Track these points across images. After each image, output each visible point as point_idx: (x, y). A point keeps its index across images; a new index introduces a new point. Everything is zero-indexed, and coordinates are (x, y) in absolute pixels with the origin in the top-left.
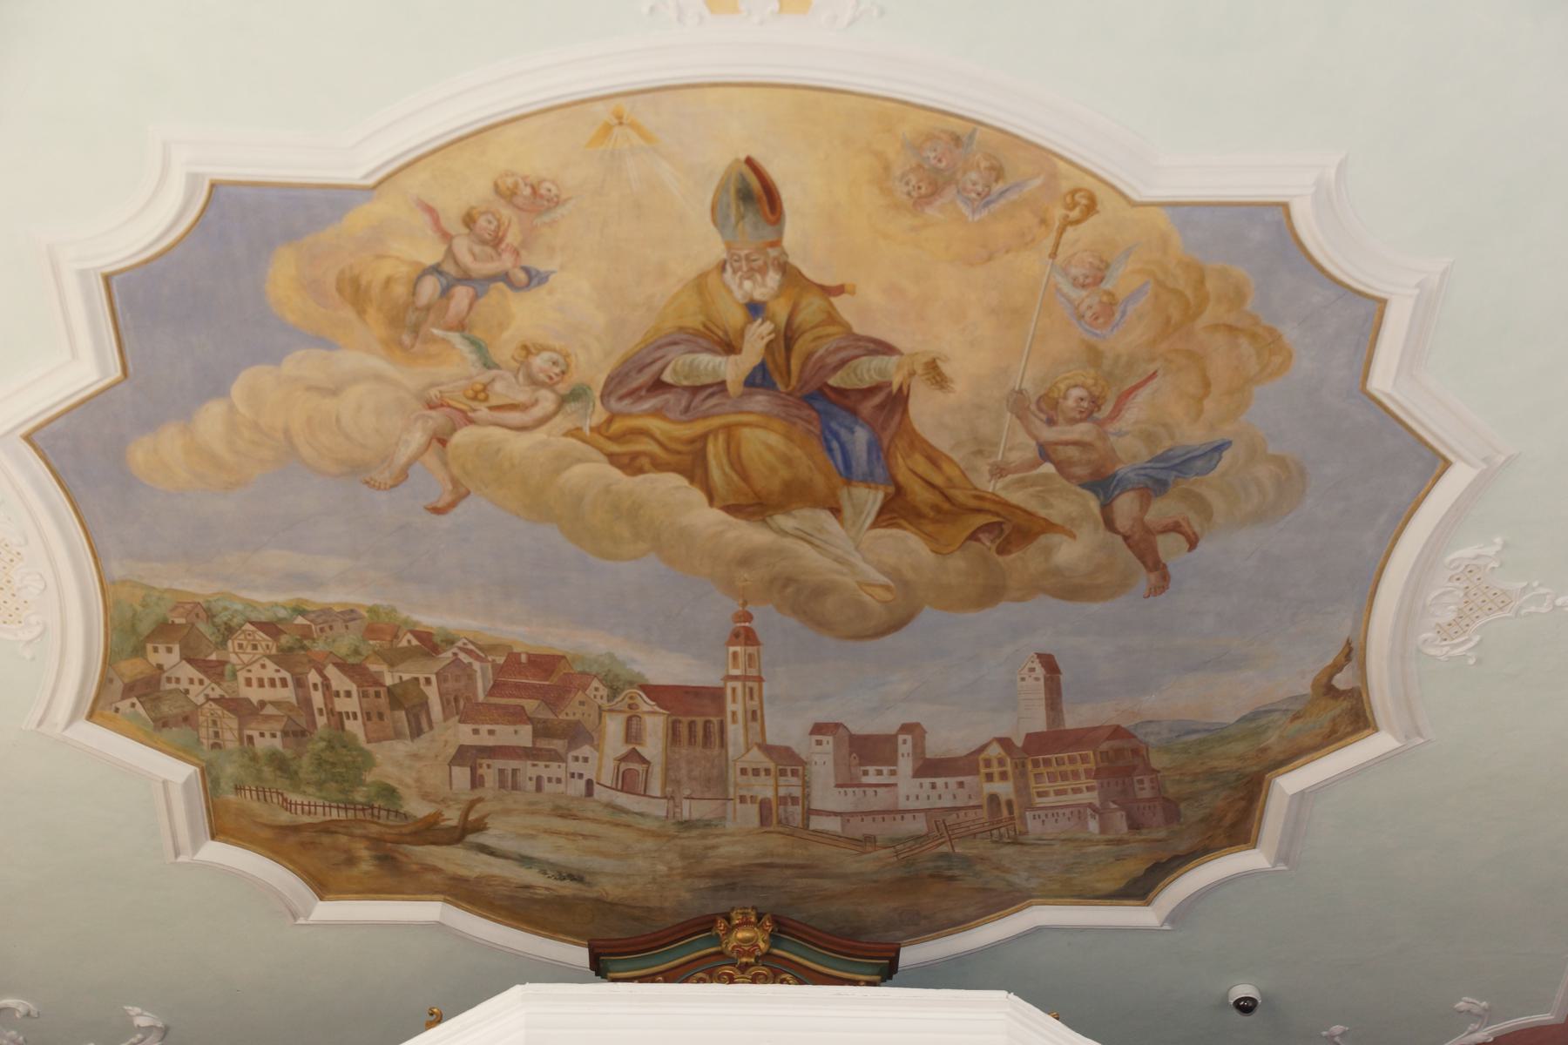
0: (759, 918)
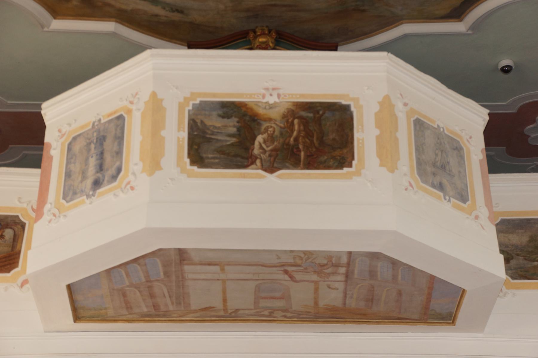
0: (270, 31)
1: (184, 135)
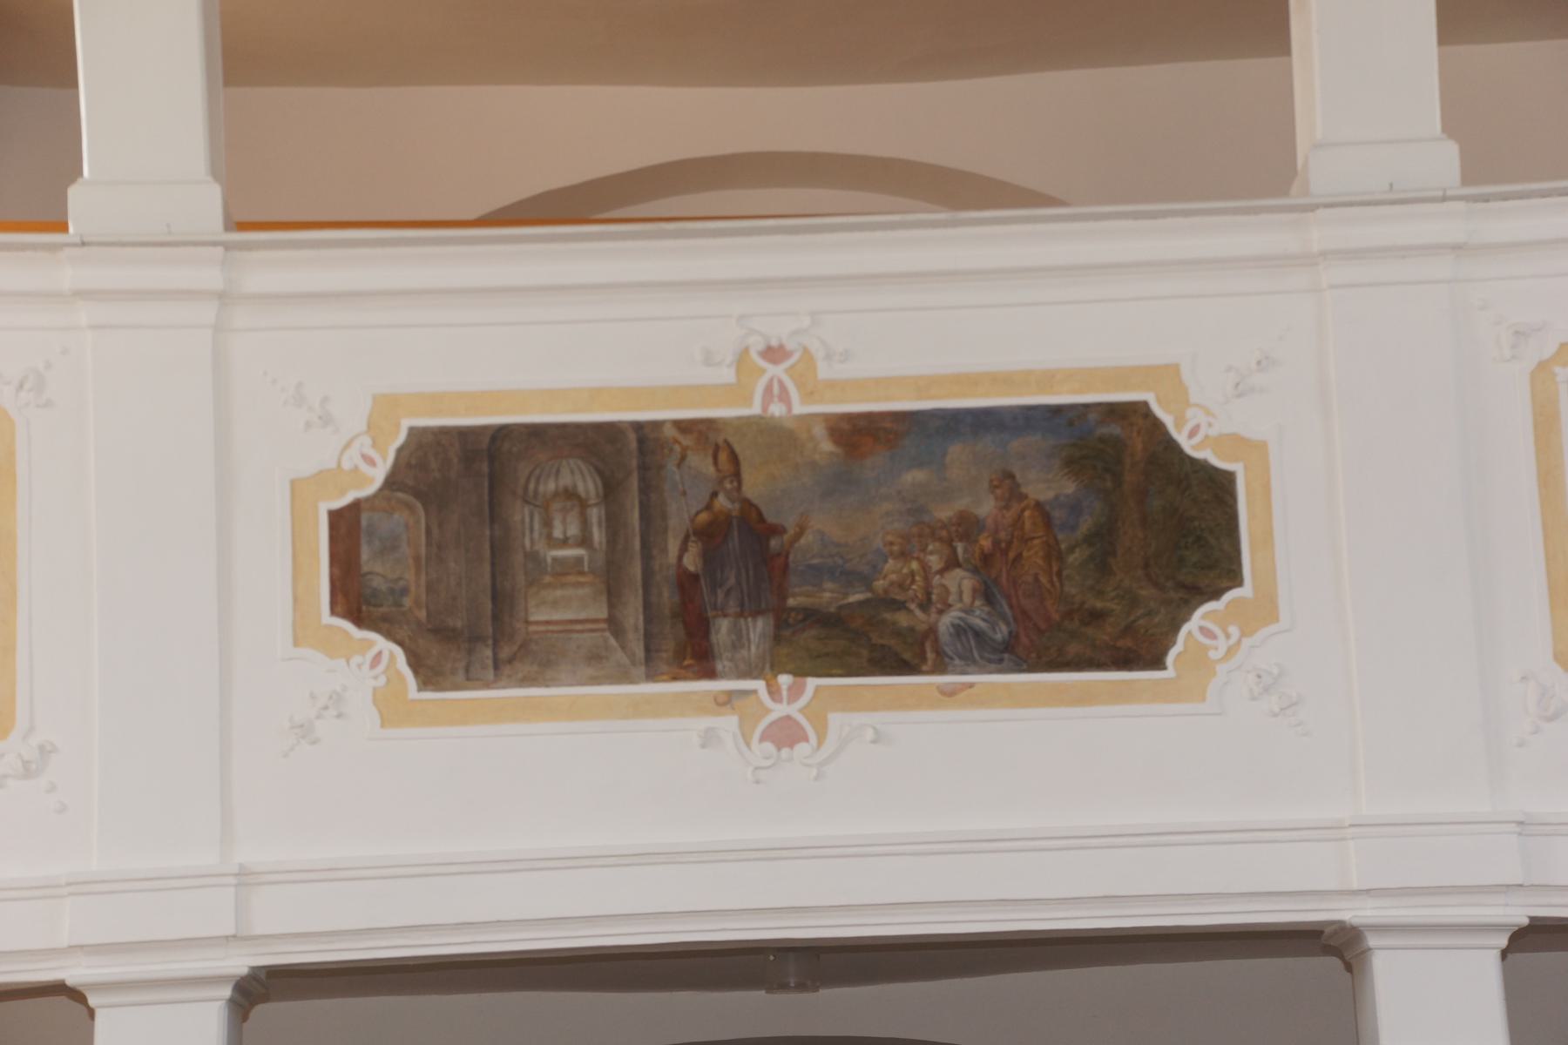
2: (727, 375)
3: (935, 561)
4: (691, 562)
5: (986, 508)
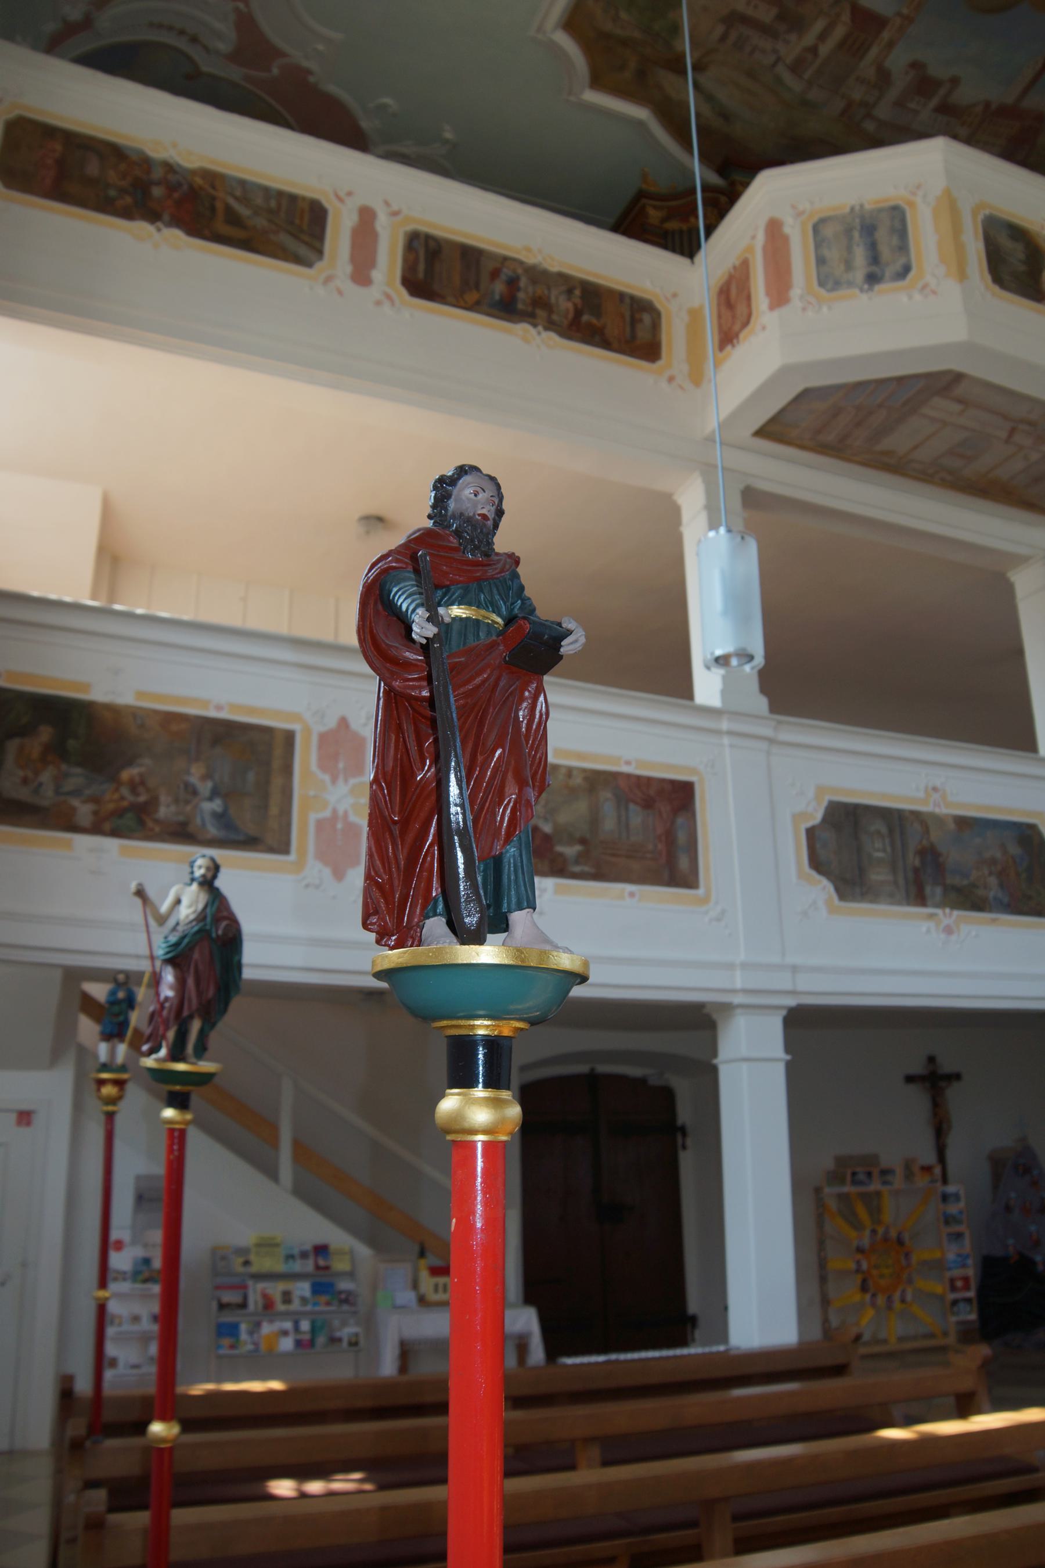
1: (981, 246)
2: (921, 794)
3: (986, 872)
4: (917, 862)
5: (998, 855)
